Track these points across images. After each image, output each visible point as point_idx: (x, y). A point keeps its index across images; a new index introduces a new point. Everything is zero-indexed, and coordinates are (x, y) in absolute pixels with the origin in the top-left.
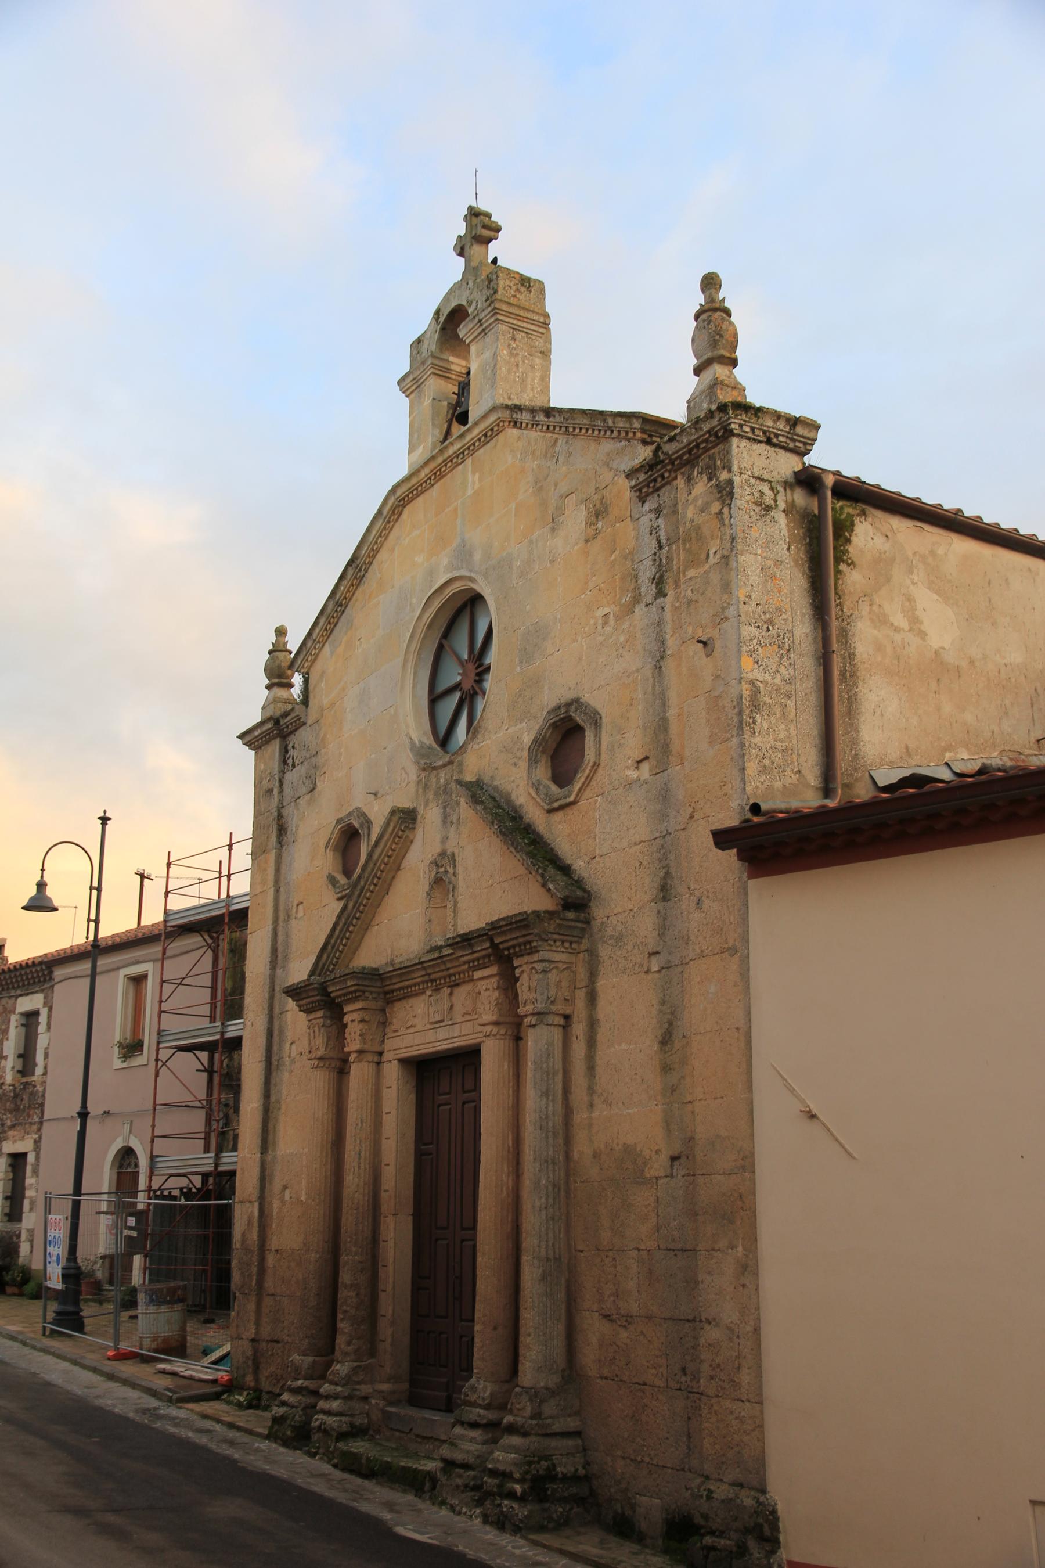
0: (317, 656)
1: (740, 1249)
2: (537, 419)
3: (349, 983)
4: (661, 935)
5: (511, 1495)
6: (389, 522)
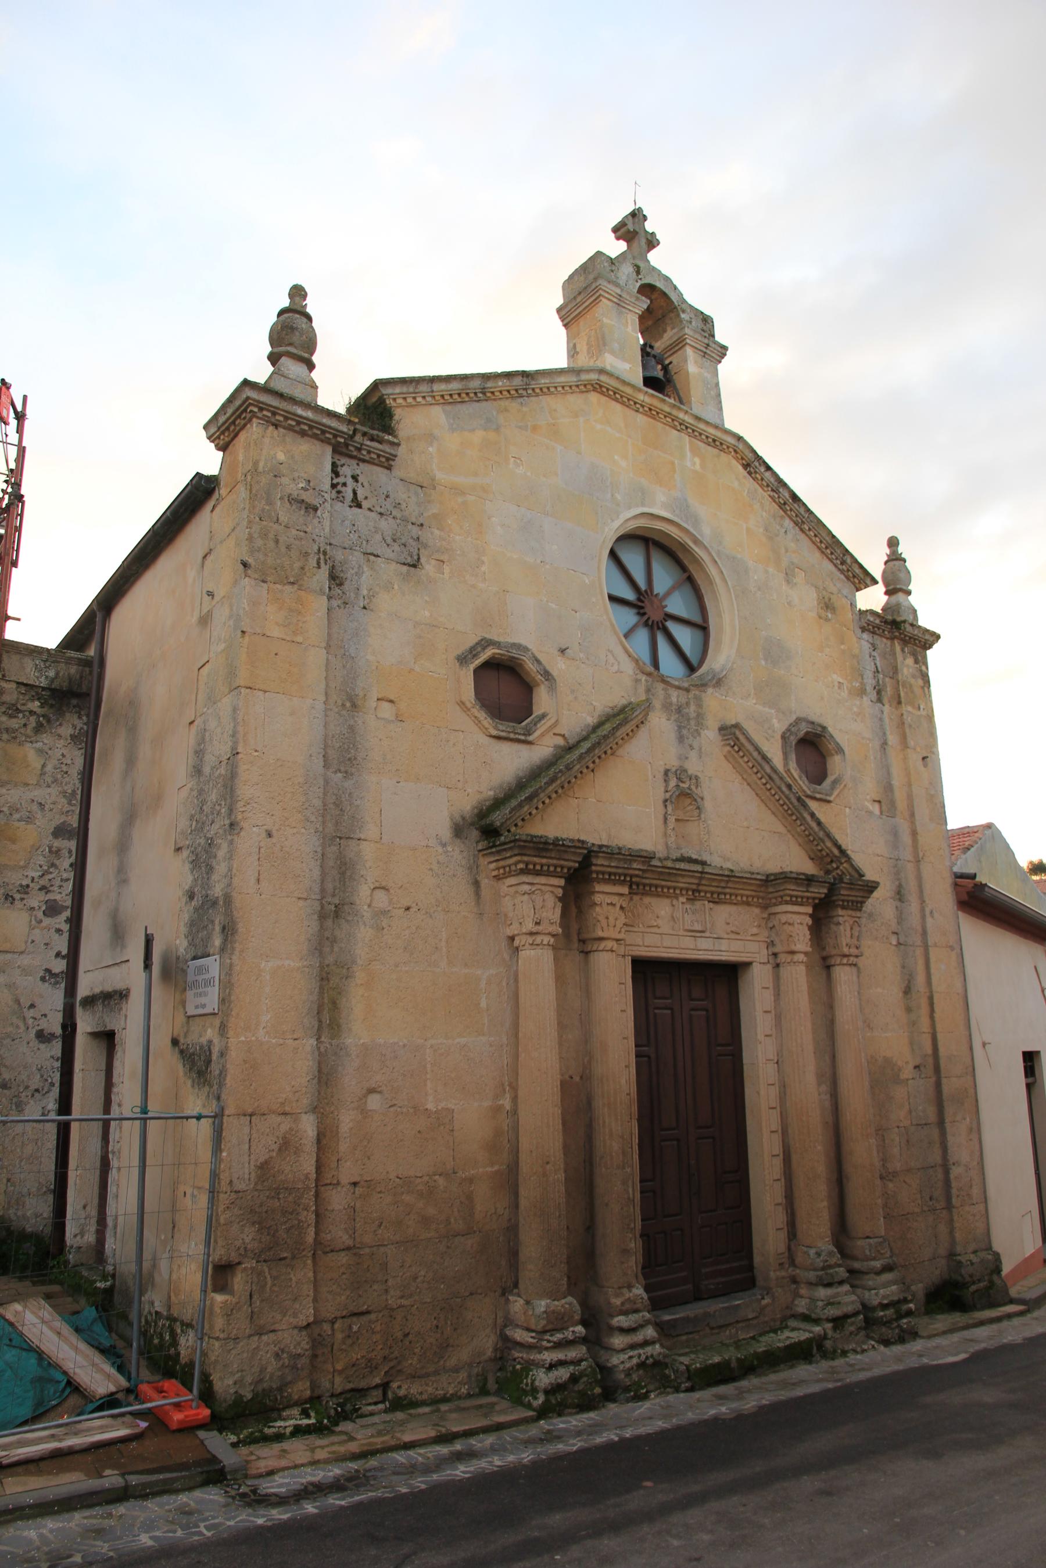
0: (419, 404)
1: (968, 1119)
2: (781, 490)
3: (635, 866)
4: (899, 923)
5: (909, 1313)
6: (577, 386)
